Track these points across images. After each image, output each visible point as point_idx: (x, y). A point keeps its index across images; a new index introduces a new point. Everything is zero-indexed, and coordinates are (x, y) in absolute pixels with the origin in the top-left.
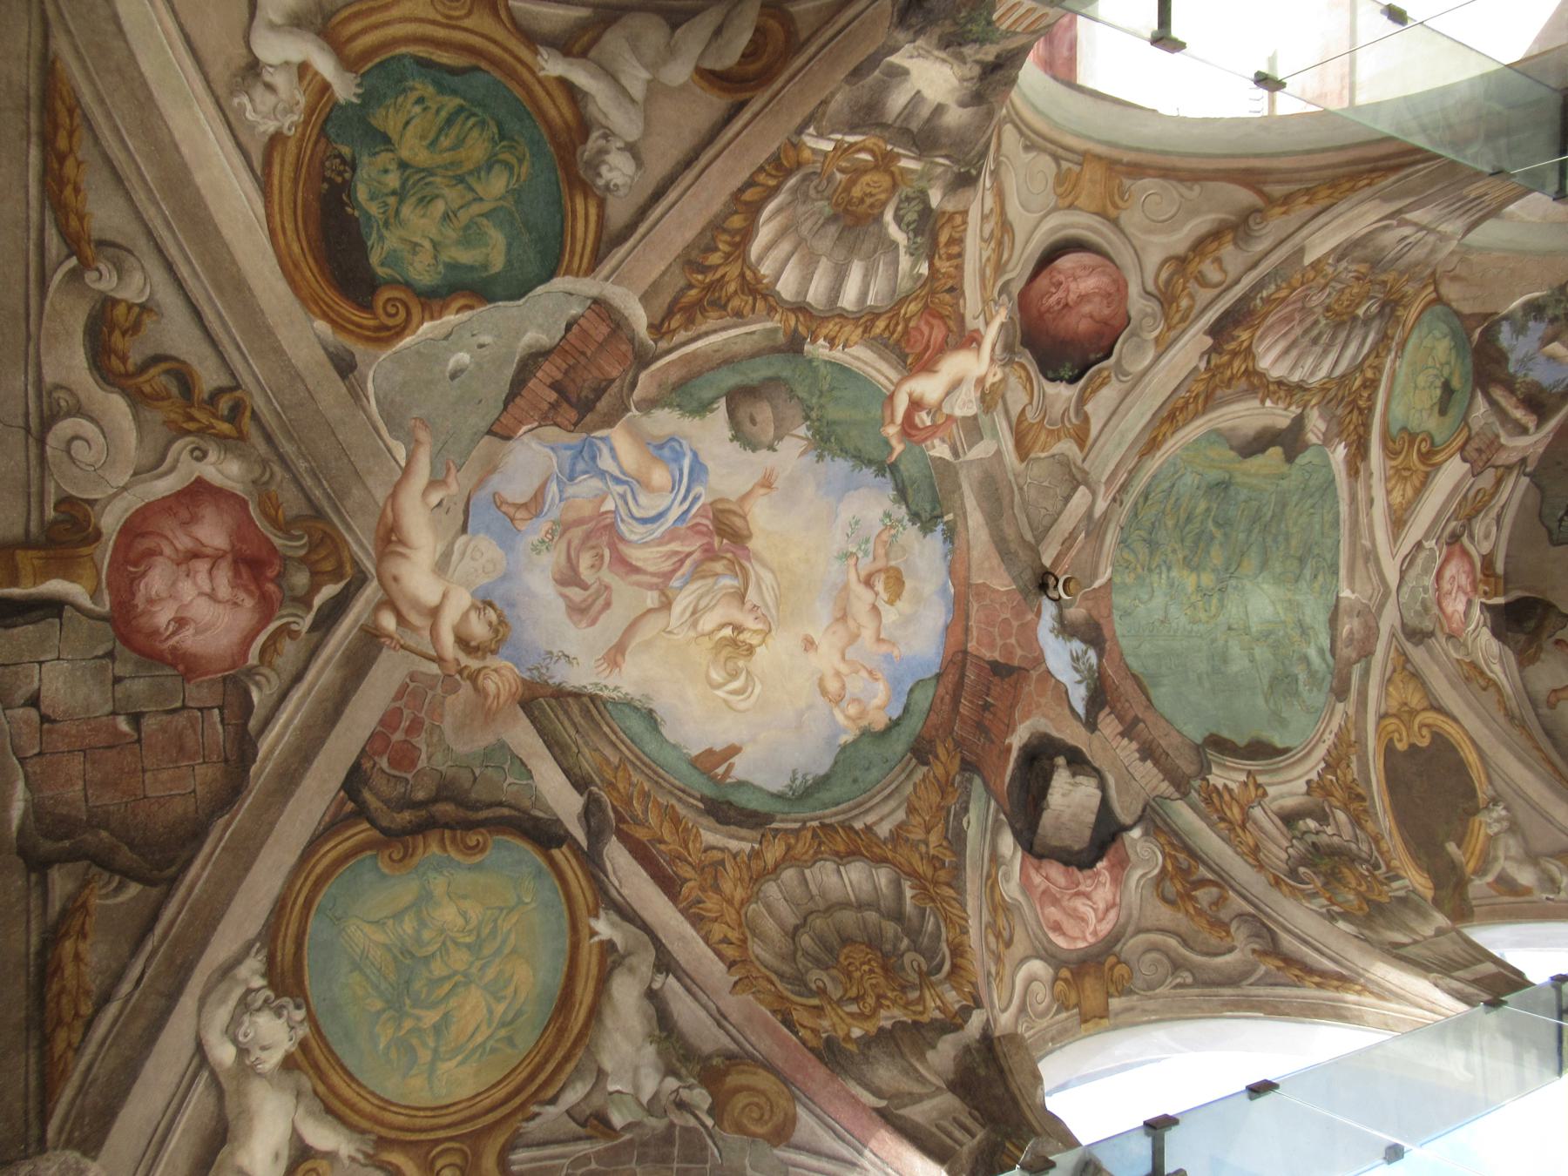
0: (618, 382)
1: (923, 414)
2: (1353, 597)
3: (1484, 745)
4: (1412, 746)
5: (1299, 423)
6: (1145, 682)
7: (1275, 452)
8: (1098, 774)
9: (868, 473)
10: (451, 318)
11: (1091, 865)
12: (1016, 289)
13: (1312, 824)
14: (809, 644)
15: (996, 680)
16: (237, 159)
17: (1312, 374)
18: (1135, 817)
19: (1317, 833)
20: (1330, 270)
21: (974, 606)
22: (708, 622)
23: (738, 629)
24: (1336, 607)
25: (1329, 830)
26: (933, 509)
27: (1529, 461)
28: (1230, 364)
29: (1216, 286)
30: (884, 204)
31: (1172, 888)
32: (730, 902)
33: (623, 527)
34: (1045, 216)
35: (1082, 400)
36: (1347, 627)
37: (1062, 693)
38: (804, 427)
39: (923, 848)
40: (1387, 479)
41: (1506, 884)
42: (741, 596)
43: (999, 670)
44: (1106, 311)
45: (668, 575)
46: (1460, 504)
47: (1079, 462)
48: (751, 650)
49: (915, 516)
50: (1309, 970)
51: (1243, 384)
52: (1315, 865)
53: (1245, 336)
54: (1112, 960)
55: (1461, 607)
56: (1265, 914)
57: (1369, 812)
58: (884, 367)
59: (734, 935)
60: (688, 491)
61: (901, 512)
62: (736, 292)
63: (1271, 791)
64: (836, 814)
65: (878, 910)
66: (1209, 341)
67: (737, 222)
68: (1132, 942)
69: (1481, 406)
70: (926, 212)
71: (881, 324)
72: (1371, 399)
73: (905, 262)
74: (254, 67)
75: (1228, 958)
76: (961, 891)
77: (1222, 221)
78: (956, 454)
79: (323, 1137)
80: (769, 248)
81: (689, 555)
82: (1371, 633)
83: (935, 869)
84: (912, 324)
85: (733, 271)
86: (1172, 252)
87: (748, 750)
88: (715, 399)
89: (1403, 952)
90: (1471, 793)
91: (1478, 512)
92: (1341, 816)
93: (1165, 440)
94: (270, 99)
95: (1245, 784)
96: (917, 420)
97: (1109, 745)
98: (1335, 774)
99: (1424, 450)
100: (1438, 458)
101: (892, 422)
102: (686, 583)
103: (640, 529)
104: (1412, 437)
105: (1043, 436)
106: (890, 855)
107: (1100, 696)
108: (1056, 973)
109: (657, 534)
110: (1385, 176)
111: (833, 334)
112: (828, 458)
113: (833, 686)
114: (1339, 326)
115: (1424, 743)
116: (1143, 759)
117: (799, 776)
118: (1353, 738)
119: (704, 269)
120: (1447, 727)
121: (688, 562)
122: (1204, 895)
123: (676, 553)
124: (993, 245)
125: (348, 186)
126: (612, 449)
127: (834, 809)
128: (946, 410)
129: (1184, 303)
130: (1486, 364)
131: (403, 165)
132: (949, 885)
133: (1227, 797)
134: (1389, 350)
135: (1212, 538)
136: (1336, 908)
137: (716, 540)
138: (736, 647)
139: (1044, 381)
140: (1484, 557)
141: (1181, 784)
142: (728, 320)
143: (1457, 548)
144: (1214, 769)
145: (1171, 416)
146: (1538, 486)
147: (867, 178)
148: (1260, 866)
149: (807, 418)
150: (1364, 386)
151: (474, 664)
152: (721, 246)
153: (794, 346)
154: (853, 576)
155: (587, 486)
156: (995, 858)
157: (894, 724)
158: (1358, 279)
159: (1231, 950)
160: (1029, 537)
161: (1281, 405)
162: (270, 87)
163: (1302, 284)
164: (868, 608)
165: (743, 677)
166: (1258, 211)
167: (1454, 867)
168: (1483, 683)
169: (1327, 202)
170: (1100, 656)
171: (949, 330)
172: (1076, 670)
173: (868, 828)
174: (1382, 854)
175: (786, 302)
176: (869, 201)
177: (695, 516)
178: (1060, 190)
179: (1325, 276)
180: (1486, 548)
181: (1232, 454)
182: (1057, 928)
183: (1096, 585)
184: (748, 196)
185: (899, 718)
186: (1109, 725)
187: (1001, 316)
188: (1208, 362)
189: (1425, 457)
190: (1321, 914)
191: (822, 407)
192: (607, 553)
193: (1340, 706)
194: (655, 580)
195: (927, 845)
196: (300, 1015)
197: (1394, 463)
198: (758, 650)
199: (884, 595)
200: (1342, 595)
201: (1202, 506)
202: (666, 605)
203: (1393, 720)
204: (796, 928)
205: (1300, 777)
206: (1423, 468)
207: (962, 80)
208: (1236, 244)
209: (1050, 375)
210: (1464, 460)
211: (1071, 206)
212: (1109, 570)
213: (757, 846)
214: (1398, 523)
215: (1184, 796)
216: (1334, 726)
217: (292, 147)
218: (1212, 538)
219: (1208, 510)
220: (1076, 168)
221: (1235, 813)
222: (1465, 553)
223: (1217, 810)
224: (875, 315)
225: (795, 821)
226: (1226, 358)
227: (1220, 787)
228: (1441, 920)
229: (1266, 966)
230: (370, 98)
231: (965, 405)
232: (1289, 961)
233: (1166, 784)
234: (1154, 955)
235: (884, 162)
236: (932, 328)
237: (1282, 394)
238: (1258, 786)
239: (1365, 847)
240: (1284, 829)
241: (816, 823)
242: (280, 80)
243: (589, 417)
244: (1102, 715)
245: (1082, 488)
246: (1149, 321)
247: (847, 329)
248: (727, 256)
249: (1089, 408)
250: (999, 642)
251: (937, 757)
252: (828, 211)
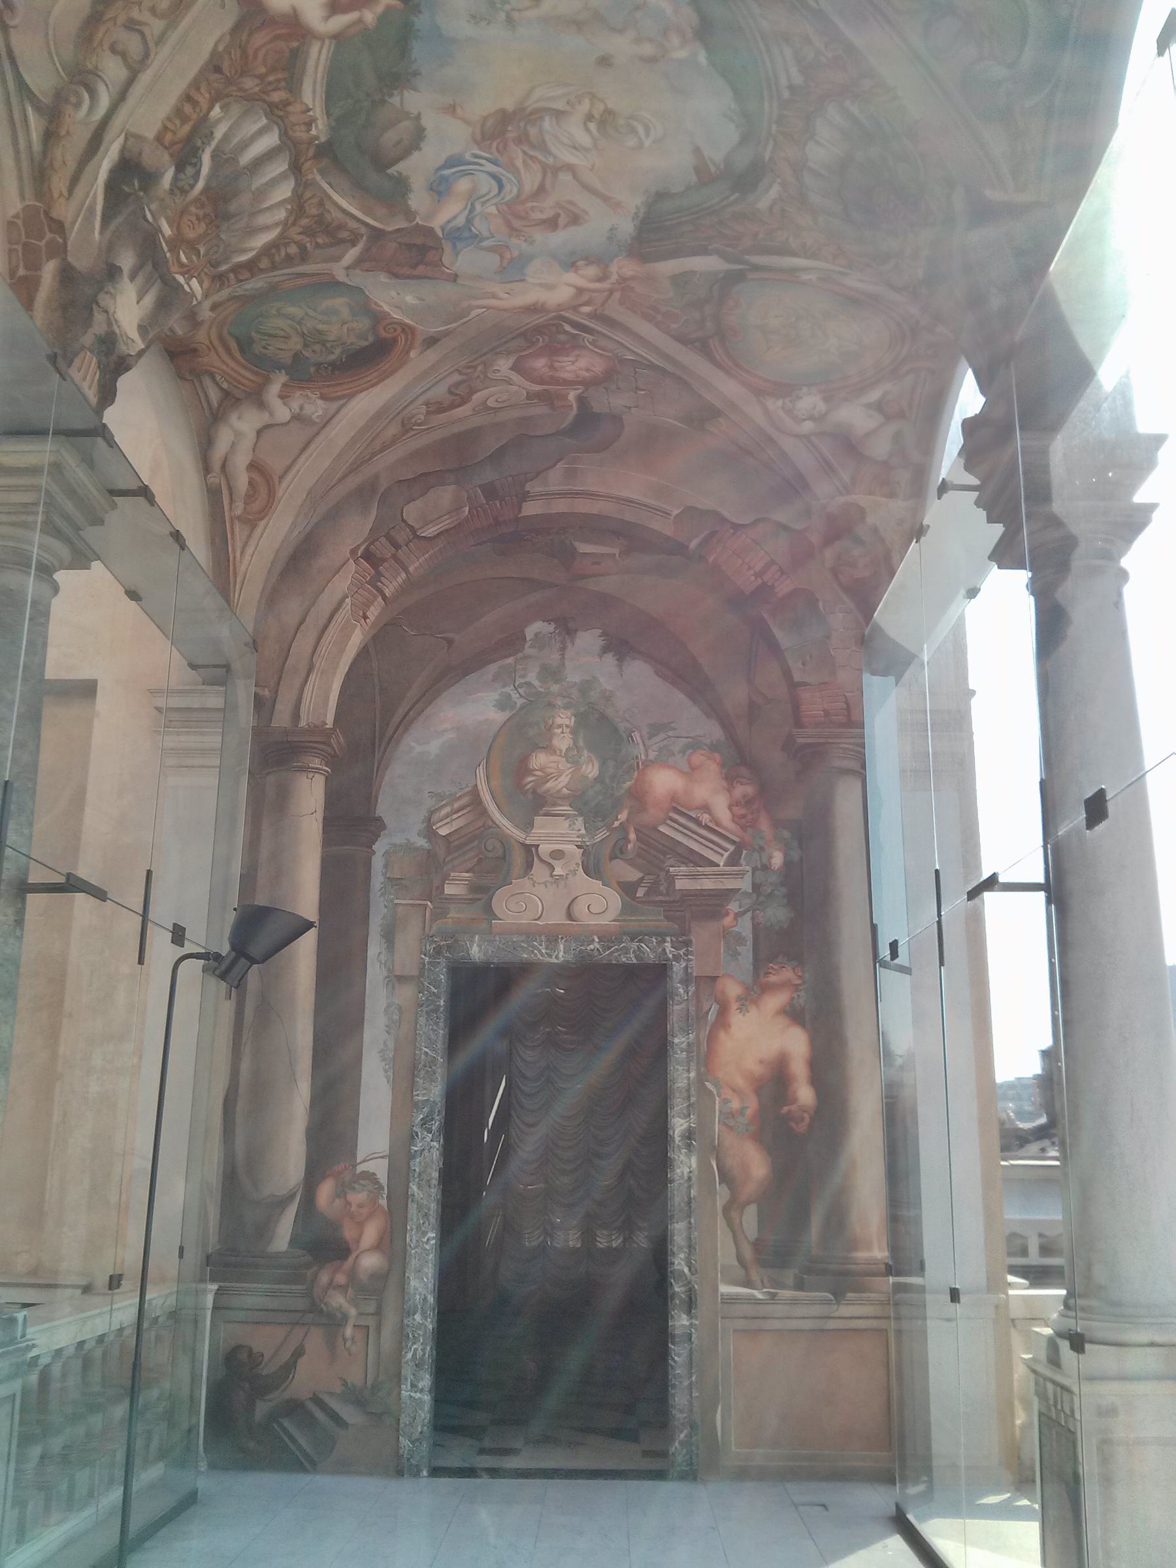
0: (399, 240)
9: (421, 22)
10: (386, 308)
16: (343, 412)
22: (584, 139)
23: (590, 117)
30: (196, 200)
33: (507, 199)
38: (392, 100)
42: (558, 114)
45: (545, 168)
48: (608, 112)
58: (311, 63)
70: (180, 168)
71: (276, 97)
73: (219, 133)
74: (296, 418)
79: (874, 395)
80: (267, 228)
81: (524, 152)
84: (263, 70)
88: (391, 177)
94: (307, 406)
101: (360, 21)
102: (550, 153)
103: (507, 188)
111: (303, 128)
113: (648, 49)
119: (303, 248)
121: (532, 153)
123: (524, 161)
125: (333, 365)
126: (449, 222)
131: (306, 346)
137: (510, 135)
138: (606, 121)
142: (329, 206)
149: (383, 102)
151: (614, 278)
152: (283, 254)
153: (327, 151)
154: (532, 13)
155: (479, 226)
162: (301, 408)
165: (635, 123)
171: (250, 34)
175: (296, 180)
176: (201, 213)
177: (491, 153)
192: (529, 205)
194: (549, 175)
196: (805, 389)
198: (610, 106)
202: (570, 168)
207: (113, 297)
213: (779, 180)
217: (325, 390)
230: (280, 367)
235: (176, 243)
236: (257, 50)
242: (295, 405)
243: (431, 244)
247: (293, 119)
248: (286, 245)
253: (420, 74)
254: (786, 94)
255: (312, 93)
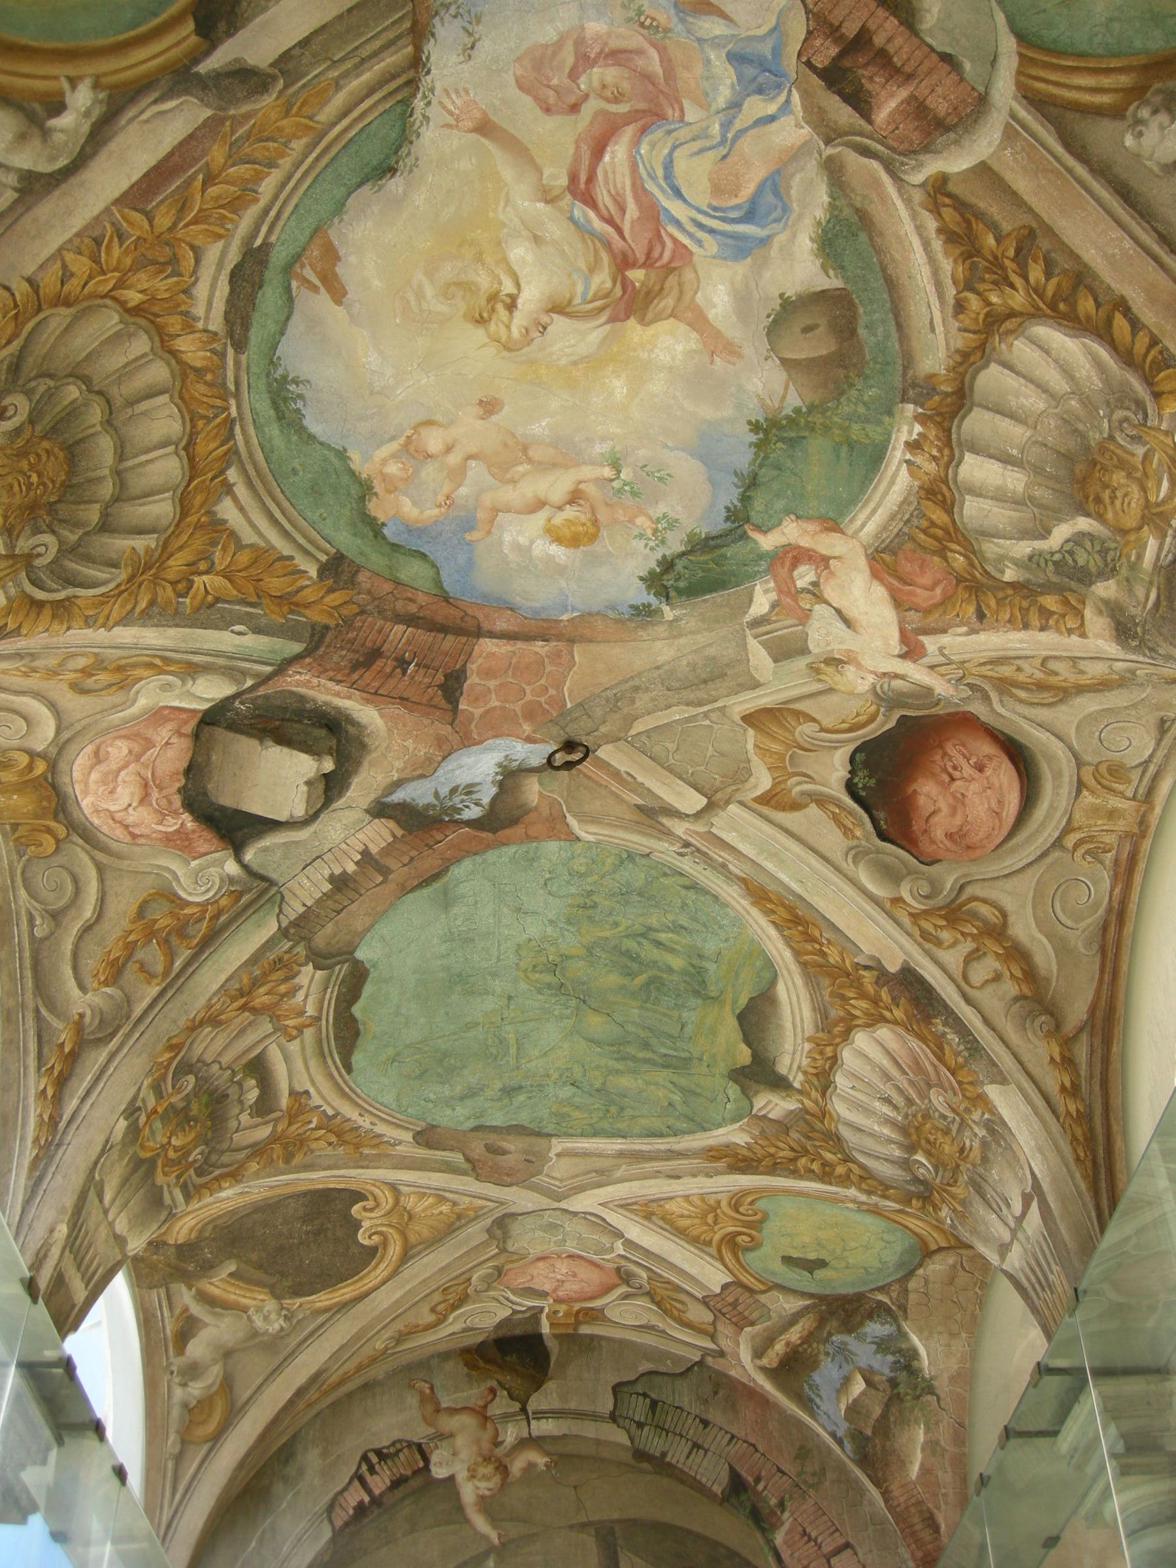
1: (811, 577)
2: (552, 1154)
3: (361, 1306)
4: (357, 1225)
5: (780, 1084)
6: (436, 885)
7: (744, 1055)
8: (311, 818)
9: (730, 496)
11: (189, 805)
12: (977, 708)
13: (252, 1095)
14: (489, 407)
15: (440, 678)
17: (844, 1099)
18: (255, 867)
19: (241, 1102)
20: (976, 1116)
21: (539, 647)
24: (539, 1134)
25: (245, 1118)
26: (677, 589)
27: (720, 1360)
28: (863, 995)
29: (965, 977)
30: (1100, 518)
31: (162, 919)
32: (121, 284)
33: (658, 134)
34: (1071, 748)
35: (821, 801)
36: (512, 1147)
37: (424, 770)
38: (798, 403)
39: (203, 566)
40: (702, 1197)
41: (187, 1330)
42: (559, 308)
43: (452, 686)
44: (939, 834)
46: (669, 1282)
47: (739, 796)
48: (481, 321)
49: (667, 565)
50: (62, 1082)
51: (835, 1013)
52: (196, 1096)
53: (898, 1014)
54: (61, 831)
55: (536, 1285)
56: (132, 1031)
57: (269, 1167)
59: (73, 286)
60: (711, 231)
61: (675, 544)
62: (988, 303)
63: (294, 1046)
64: (247, 442)
65: (116, 499)
66: (893, 968)
67: (1086, 305)
68: (85, 858)
69: (792, 1305)
70: (1085, 577)
72: (810, 1174)
73: (1024, 548)
75: (72, 983)
76: (146, 618)
77: (1048, 980)
78: (757, 623)
82: (502, 1177)
83: (173, 584)
85: (1018, 299)
86: (1012, 919)
87: (340, 311)
89: (92, 1195)
90: (297, 1292)
91: (658, 1304)
92: (264, 1132)
93: (767, 913)
95: (302, 1013)
96: (802, 569)
97: (350, 831)
98: (317, 1128)
99: (739, 1239)
100: (728, 1257)
104: (757, 1225)
105: (776, 747)
106: (192, 519)
107: (417, 823)
108: (39, 755)
109: (650, 186)
110: (1084, 1177)
112: (753, 438)
114: (904, 1130)
115: (362, 1238)
116: (332, 879)
117: (301, 389)
118: (366, 1151)
119: (1022, 256)
120: (382, 1266)
121: (609, 229)
122: (153, 955)
123: (623, 210)
124: (1039, 675)
127: (255, 441)
128: (819, 608)
129: (945, 935)
130: (844, 1311)
132: (152, 603)
133: (283, 988)
134: (869, 1193)
135: (631, 974)
136: (143, 1119)
139: (851, 747)
140: (601, 1310)
141: (299, 929)
142: (951, 292)
143: (615, 1280)
144: (319, 974)
145: (797, 921)
146: (690, 1369)
147: (1135, 491)
148: (194, 1027)
150: (825, 1164)
154: (587, 472)
156: (192, 671)
157: (375, 528)
158: (962, 1150)
159: (82, 988)
160: (639, 727)
161: (805, 1062)
163: (960, 1083)
164: (542, 495)
166: (1058, 1026)
167: (207, 1268)
168: (440, 1308)
169: (1062, 1110)
170: (469, 823)
172: (454, 791)
173: (228, 489)
174: (217, 1179)
178: (1103, 769)
179: (968, 1110)
180: (613, 1314)
181: (743, 1001)
182: (98, 758)
183: (570, 819)
184: (1120, 324)
185: (384, 538)
186: (378, 834)
187: (941, 687)
188: (866, 968)
189: (730, 1240)
190: (135, 1098)
191: (827, 429)
192: (623, 108)
193: (408, 1136)
195: (207, 572)
197: (724, 1204)
199: (558, 519)
200: (554, 1141)
201: (677, 963)
203: (391, 1201)
204: (86, 380)
205: (313, 1083)
206: (717, 1237)
208: (1016, 999)
209: (860, 757)
210: (725, 1287)
211: (1080, 785)
212: (591, 838)
214: (648, 1211)
215: (284, 932)
216: (381, 1129)
218: (631, 974)
219: (670, 970)
220: (1130, 794)
221: (261, 998)
222: (608, 1289)
223: (265, 974)
224: (948, 507)
225: (237, 384)
226: (871, 989)
227: (297, 980)
228: (136, 1244)
229: (65, 1036)
231: (823, 633)
232: (73, 1058)
233: (302, 910)
234: (70, 888)
237: (819, 1063)
238: (300, 1029)
239: (225, 1159)
240: (244, 1061)
241: (234, 412)
244: (391, 824)
245: (704, 801)
246: (925, 889)
248: (1039, 292)
249: (813, 809)
250: (492, 684)
251: (331, 590)
252: (1095, 437)
253: (749, 423)
254: (232, 475)
255: (896, 483)
